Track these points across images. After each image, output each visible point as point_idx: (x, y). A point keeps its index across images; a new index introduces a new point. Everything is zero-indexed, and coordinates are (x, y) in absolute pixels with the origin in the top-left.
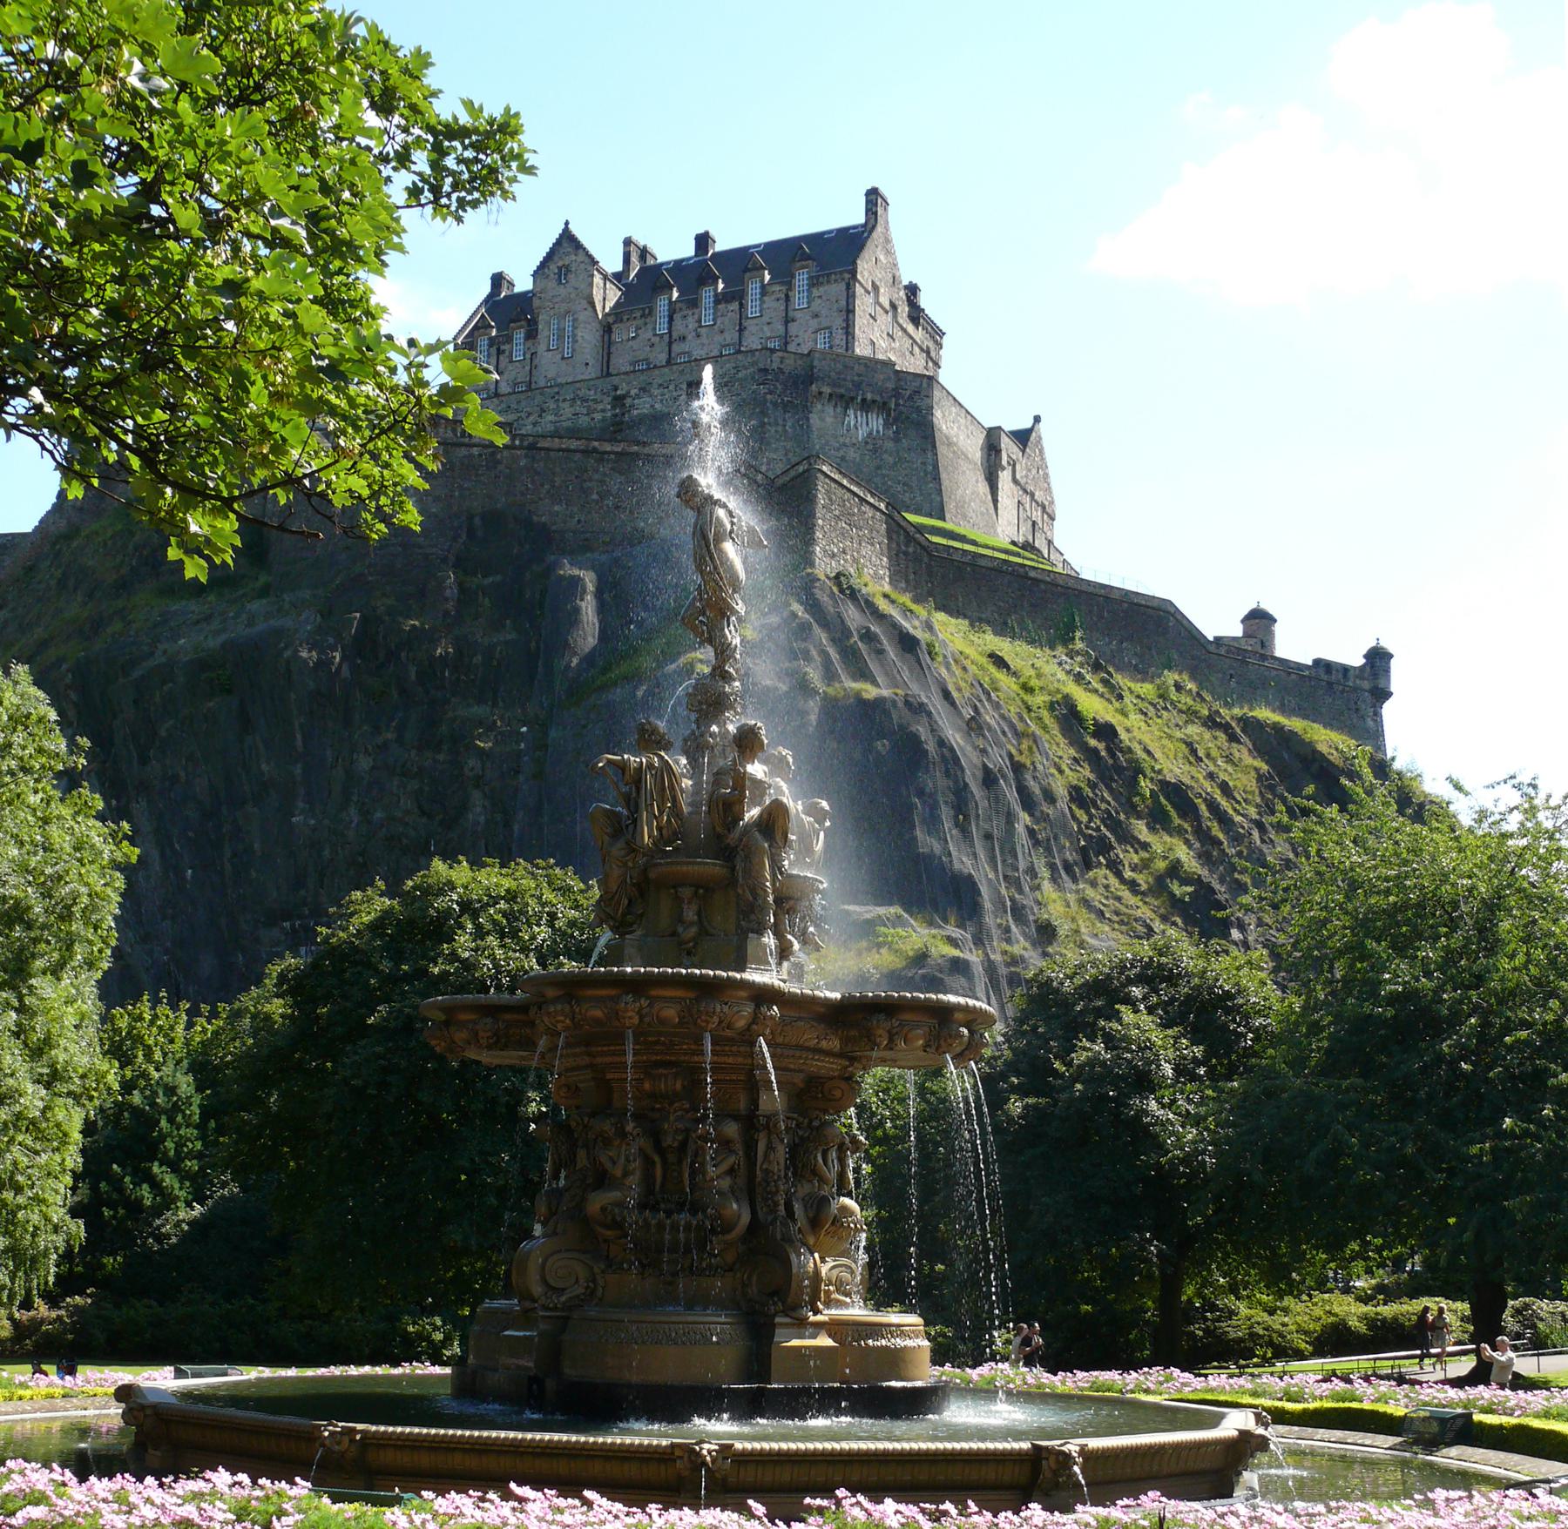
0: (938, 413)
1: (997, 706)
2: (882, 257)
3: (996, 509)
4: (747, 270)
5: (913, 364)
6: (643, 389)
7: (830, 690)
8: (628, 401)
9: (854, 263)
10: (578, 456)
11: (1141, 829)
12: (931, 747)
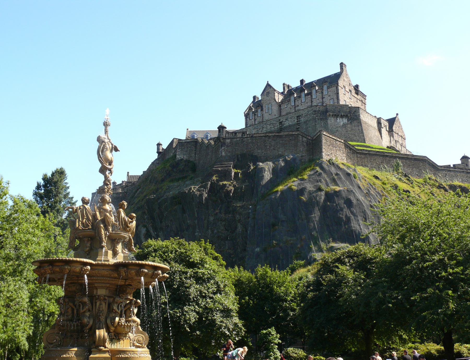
0: (362, 116)
1: (375, 189)
2: (345, 79)
4: (312, 87)
5: (359, 104)
6: (286, 120)
7: (327, 190)
8: (283, 123)
9: (338, 82)
10: (263, 138)
12: (354, 202)
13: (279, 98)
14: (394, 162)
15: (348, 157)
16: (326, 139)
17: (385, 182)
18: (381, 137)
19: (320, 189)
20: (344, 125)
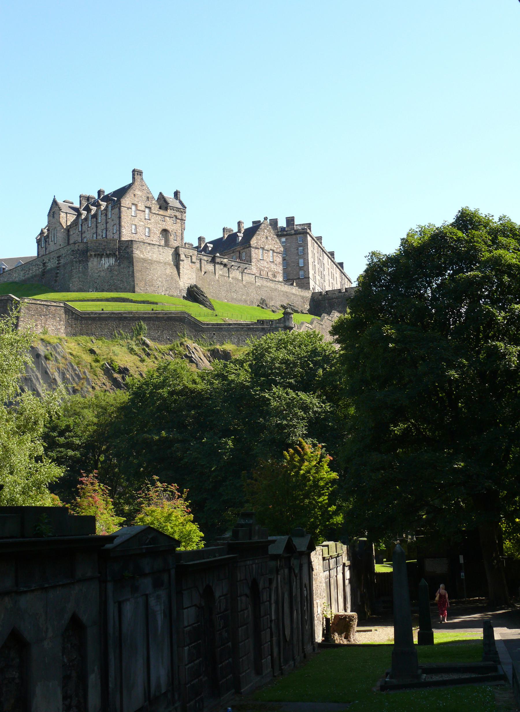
3: (179, 275)
8: (46, 264)
13: (67, 219)
14: (134, 326)
15: (68, 325)
20: (110, 269)
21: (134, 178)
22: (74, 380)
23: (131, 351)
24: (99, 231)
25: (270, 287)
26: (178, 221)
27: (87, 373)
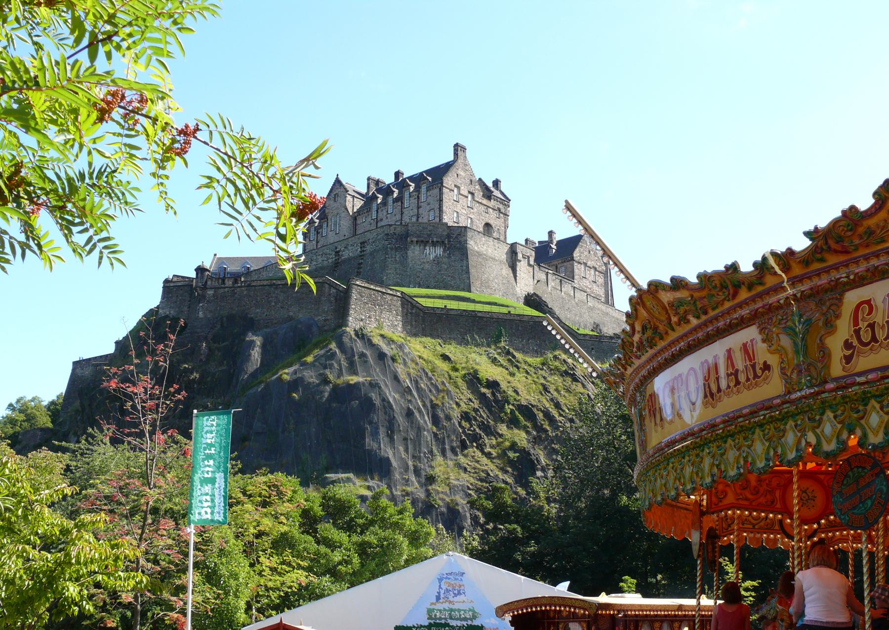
2: (462, 173)
4: (404, 187)
11: (503, 429)
12: (377, 402)
13: (354, 205)
16: (360, 293)
17: (458, 366)
18: (515, 277)
19: (325, 381)
20: (437, 261)
21: (456, 154)
22: (430, 391)
23: (494, 361)
24: (406, 219)
25: (602, 311)
26: (502, 215)
27: (447, 385)
